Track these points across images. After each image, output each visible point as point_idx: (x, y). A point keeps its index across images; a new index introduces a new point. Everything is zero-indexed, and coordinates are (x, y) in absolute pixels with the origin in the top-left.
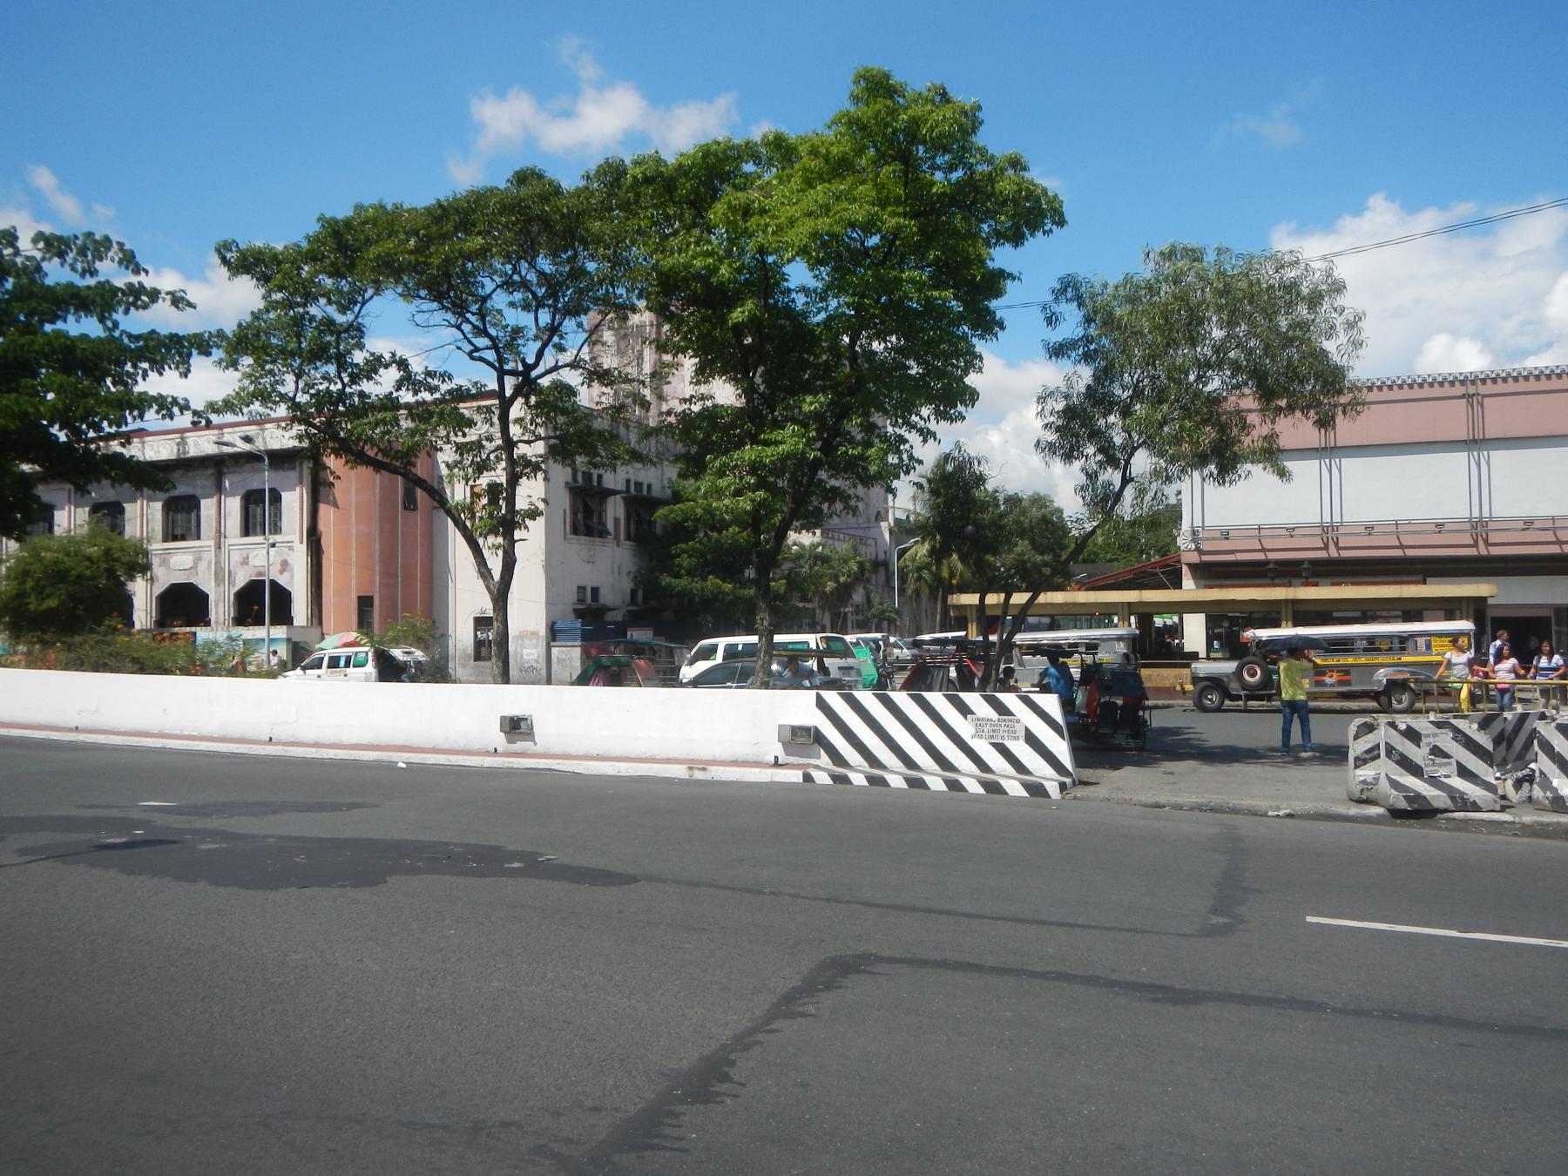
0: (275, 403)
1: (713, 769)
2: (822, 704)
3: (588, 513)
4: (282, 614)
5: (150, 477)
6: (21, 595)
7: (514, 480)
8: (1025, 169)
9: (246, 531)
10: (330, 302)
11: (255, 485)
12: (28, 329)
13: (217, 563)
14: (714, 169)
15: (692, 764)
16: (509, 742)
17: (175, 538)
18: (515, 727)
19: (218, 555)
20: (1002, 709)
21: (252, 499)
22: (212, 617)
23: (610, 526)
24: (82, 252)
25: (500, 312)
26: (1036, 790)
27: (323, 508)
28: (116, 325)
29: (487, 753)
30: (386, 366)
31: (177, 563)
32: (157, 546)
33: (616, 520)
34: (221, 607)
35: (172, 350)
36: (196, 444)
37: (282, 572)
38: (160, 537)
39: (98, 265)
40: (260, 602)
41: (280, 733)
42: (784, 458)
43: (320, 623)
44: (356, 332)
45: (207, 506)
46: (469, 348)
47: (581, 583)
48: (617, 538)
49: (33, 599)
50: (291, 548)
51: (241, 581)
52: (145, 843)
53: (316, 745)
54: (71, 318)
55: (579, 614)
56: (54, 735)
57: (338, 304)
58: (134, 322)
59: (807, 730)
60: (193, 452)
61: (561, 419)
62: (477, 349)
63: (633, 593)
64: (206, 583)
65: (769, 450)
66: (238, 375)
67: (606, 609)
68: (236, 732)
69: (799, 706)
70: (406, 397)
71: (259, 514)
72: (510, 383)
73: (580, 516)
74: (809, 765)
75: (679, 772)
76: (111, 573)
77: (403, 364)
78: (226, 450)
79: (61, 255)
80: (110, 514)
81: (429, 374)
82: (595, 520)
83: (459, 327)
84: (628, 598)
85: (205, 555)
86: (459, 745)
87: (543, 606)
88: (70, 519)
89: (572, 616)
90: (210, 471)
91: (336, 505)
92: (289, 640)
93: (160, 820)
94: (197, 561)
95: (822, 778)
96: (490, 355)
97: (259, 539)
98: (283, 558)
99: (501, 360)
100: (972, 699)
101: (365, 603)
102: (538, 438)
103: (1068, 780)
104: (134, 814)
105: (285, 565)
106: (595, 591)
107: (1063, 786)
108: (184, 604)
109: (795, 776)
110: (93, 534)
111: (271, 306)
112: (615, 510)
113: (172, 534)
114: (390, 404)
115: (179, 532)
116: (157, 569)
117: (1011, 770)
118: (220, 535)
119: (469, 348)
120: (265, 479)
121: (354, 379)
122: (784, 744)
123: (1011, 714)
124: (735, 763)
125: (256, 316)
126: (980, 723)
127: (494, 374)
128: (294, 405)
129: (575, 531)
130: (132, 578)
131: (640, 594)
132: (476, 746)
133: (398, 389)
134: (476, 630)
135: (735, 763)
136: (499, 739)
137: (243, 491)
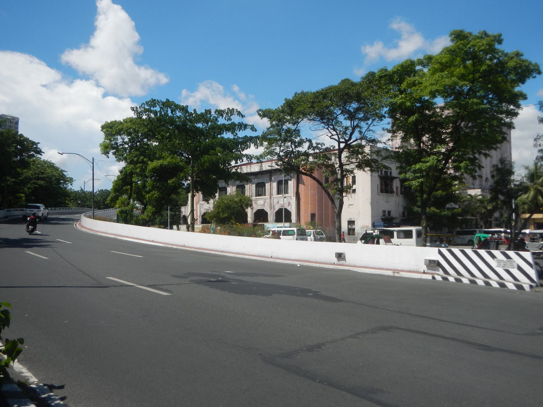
0: (275, 155)
1: (401, 273)
2: (440, 253)
3: (386, 185)
4: (288, 219)
5: (246, 178)
6: (218, 213)
7: (343, 176)
8: (522, 55)
9: (279, 192)
10: (289, 123)
11: (281, 179)
12: (214, 137)
13: (270, 203)
14: (407, 69)
15: (394, 271)
16: (339, 261)
17: (259, 195)
18: (340, 256)
19: (270, 200)
20: (508, 257)
21: (279, 183)
22: (269, 219)
23: (395, 190)
24: (227, 114)
25: (341, 122)
26: (520, 287)
27: (300, 185)
28: (237, 134)
29: (331, 264)
30: (305, 142)
31: (259, 203)
32: (254, 198)
33: (397, 187)
34: (271, 216)
35: (246, 142)
36: (265, 167)
39: (232, 117)
40: (282, 215)
41: (274, 255)
42: (430, 167)
43: (300, 222)
44: (297, 132)
45: (267, 185)
46: (330, 135)
47: (384, 209)
48: (397, 193)
50: (291, 198)
52: (220, 281)
53: (283, 259)
54: (225, 133)
55: (383, 220)
56: (217, 253)
57: (292, 123)
58: (241, 134)
59: (434, 261)
60: (264, 169)
61: (360, 156)
62: (333, 135)
63: (403, 213)
64: (267, 209)
65: (424, 165)
66: (263, 148)
67: (393, 219)
68: (262, 254)
69: (432, 253)
70: (311, 151)
71: (282, 188)
72: (342, 145)
73: (383, 186)
74: (435, 274)
75: (390, 273)
76: (242, 206)
77: (310, 141)
78: (273, 168)
79: (222, 115)
80: (241, 188)
81: (317, 144)
82: (389, 187)
83: (328, 129)
84: (402, 215)
85: (267, 201)
86: (324, 261)
87: (370, 217)
88: (231, 190)
89: (381, 221)
90: (268, 175)
91: (304, 185)
93: (227, 276)
94: (265, 202)
95: (438, 278)
96: (336, 137)
97: (281, 196)
98: (288, 200)
99: (339, 138)
100: (495, 252)
101: (313, 216)
102: (352, 163)
103: (533, 284)
104: (222, 274)
105: (289, 203)
106: (389, 212)
107: (531, 287)
108: (261, 216)
109: (429, 277)
110: (237, 195)
111: (272, 126)
112: (396, 184)
113: (258, 194)
114: (307, 154)
115: (260, 193)
116: (254, 205)
117: (512, 280)
118: (271, 194)
119: (330, 135)
120: (282, 177)
121: (296, 147)
122: (427, 266)
123: (511, 259)
124: (410, 271)
125: (268, 129)
126: (499, 261)
127: (337, 143)
128: (279, 156)
129: (382, 191)
130: (247, 208)
131: (406, 213)
132: (328, 262)
133: (308, 149)
134: (348, 225)
135: (410, 271)
136: (335, 260)
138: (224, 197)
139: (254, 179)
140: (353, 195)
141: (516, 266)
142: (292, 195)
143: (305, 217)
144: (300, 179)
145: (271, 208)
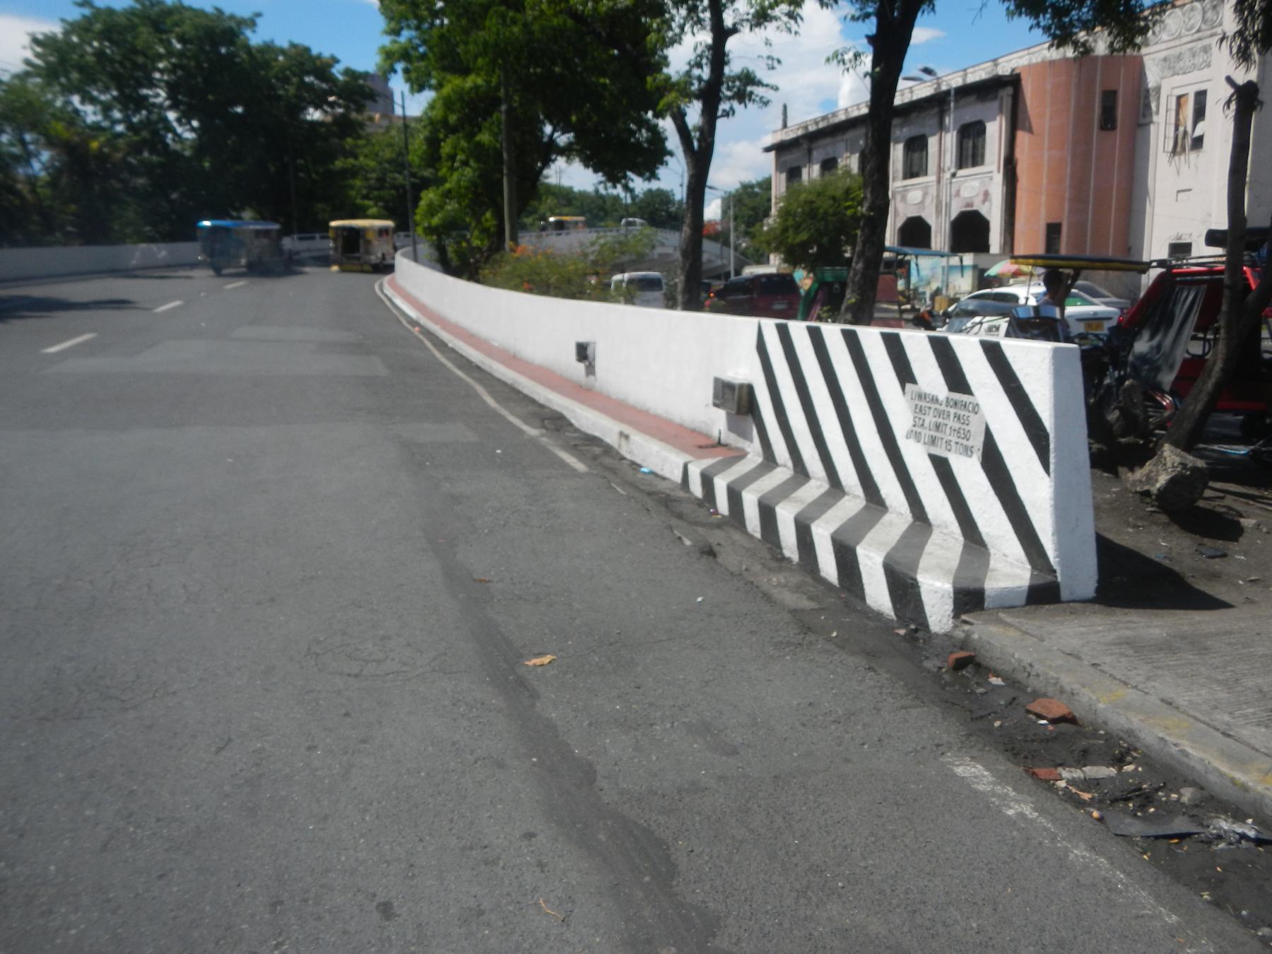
4: (980, 245)
9: (961, 164)
13: (938, 196)
34: (940, 239)
37: (984, 201)
38: (900, 174)
45: (933, 142)
49: (791, 233)
51: (954, 215)
64: (931, 219)
90: (936, 110)
91: (1030, 131)
92: (975, 267)
94: (925, 194)
98: (981, 188)
105: (986, 195)
115: (915, 169)
120: (971, 112)
137: (958, 126)
138: (796, 185)
139: (902, 126)
140: (1193, 156)
141: (978, 442)
142: (994, 167)
143: (1030, 239)
144: (1020, 117)
145: (938, 212)
